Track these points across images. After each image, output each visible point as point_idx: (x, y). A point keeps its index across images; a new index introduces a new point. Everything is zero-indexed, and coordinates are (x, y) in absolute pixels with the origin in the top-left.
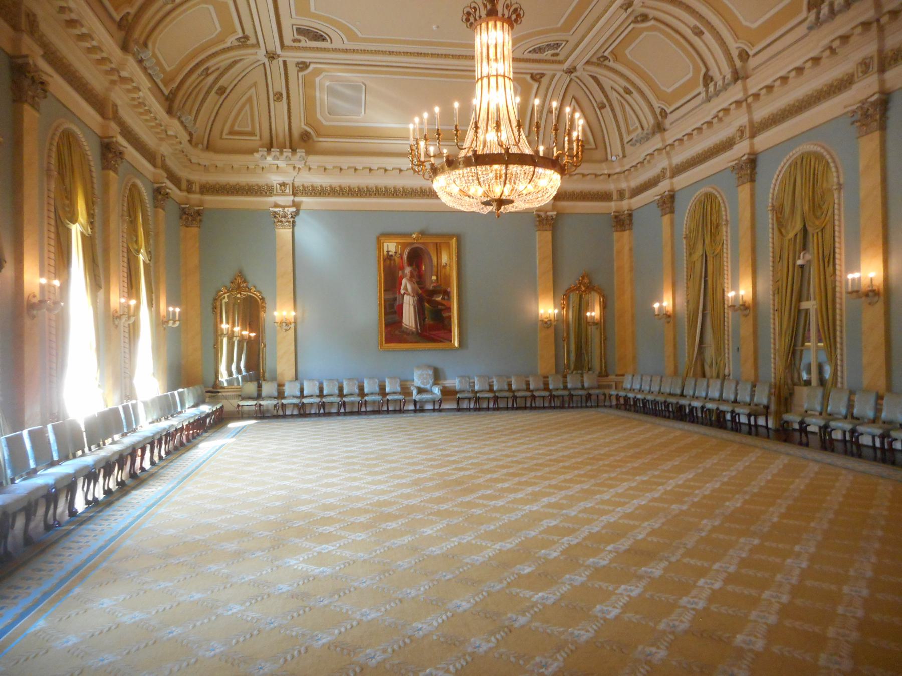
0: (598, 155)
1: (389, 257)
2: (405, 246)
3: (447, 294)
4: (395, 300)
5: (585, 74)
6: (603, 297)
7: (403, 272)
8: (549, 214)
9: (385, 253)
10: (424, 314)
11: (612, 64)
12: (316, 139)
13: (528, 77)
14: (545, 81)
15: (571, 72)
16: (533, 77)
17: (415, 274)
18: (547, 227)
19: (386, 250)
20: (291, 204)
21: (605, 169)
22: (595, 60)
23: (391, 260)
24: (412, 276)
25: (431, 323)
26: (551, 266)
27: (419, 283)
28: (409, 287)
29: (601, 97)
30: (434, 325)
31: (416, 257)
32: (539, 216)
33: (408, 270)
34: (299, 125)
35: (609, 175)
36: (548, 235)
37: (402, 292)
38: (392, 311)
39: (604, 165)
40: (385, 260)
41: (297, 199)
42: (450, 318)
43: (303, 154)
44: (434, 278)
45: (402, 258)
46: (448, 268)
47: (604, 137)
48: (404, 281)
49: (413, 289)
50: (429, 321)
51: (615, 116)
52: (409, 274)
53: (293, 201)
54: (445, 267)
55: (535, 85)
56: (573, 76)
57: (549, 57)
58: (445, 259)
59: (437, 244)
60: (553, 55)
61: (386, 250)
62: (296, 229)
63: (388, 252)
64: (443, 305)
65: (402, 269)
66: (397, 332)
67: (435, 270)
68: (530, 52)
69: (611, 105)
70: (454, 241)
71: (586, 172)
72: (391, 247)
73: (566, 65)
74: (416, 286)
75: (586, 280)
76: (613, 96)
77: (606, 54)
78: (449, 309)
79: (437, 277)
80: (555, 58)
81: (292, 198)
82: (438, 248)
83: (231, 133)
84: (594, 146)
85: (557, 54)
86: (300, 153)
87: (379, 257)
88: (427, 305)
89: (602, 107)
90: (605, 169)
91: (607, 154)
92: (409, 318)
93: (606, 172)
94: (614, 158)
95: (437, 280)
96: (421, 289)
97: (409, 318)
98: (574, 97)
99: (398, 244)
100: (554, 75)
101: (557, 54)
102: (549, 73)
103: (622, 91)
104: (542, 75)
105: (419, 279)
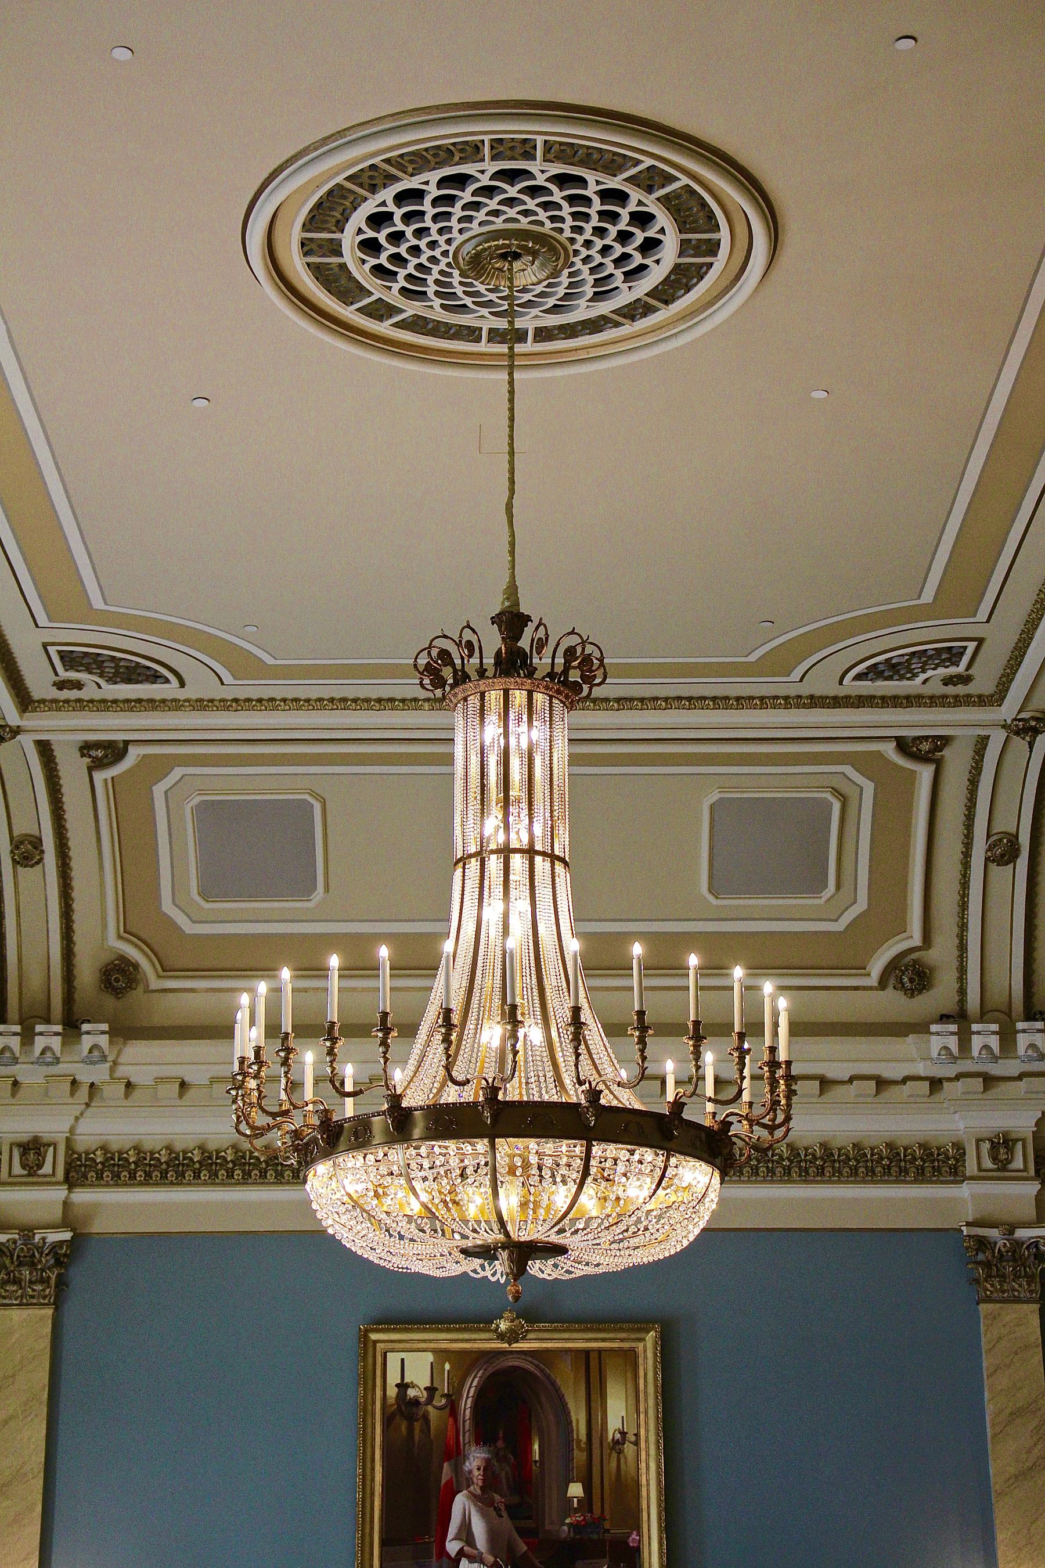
1: (405, 1408)
2: (467, 1362)
7: (457, 1469)
8: (1021, 1233)
9: (392, 1392)
12: (155, 984)
13: (889, 749)
14: (957, 762)
16: (903, 745)
17: (504, 1472)
18: (1021, 1287)
19: (393, 1378)
20: (58, 1214)
23: (411, 1419)
24: (490, 1481)
27: (514, 1511)
28: (479, 1528)
31: (511, 1402)
32: (982, 1243)
33: (475, 1460)
34: (101, 937)
37: (453, 1547)
40: (388, 1421)
41: (82, 1196)
43: (103, 1040)
44: (576, 1490)
46: (629, 1449)
48: (460, 1503)
53: (66, 1204)
54: (618, 1445)
55: (925, 773)
57: (936, 688)
58: (616, 1412)
59: (587, 1353)
60: (948, 681)
61: (393, 1378)
63: (403, 1386)
65: (455, 1454)
67: (579, 1456)
68: (859, 677)
70: (648, 1345)
72: (413, 1365)
73: (1008, 710)
74: (506, 1523)
79: (588, 1488)
80: (960, 690)
81: (60, 1193)
82: (592, 1368)
85: (965, 679)
86: (94, 1035)
87: (365, 1411)
96: (522, 1532)
99: (442, 1355)
100: (983, 742)
101: (965, 679)
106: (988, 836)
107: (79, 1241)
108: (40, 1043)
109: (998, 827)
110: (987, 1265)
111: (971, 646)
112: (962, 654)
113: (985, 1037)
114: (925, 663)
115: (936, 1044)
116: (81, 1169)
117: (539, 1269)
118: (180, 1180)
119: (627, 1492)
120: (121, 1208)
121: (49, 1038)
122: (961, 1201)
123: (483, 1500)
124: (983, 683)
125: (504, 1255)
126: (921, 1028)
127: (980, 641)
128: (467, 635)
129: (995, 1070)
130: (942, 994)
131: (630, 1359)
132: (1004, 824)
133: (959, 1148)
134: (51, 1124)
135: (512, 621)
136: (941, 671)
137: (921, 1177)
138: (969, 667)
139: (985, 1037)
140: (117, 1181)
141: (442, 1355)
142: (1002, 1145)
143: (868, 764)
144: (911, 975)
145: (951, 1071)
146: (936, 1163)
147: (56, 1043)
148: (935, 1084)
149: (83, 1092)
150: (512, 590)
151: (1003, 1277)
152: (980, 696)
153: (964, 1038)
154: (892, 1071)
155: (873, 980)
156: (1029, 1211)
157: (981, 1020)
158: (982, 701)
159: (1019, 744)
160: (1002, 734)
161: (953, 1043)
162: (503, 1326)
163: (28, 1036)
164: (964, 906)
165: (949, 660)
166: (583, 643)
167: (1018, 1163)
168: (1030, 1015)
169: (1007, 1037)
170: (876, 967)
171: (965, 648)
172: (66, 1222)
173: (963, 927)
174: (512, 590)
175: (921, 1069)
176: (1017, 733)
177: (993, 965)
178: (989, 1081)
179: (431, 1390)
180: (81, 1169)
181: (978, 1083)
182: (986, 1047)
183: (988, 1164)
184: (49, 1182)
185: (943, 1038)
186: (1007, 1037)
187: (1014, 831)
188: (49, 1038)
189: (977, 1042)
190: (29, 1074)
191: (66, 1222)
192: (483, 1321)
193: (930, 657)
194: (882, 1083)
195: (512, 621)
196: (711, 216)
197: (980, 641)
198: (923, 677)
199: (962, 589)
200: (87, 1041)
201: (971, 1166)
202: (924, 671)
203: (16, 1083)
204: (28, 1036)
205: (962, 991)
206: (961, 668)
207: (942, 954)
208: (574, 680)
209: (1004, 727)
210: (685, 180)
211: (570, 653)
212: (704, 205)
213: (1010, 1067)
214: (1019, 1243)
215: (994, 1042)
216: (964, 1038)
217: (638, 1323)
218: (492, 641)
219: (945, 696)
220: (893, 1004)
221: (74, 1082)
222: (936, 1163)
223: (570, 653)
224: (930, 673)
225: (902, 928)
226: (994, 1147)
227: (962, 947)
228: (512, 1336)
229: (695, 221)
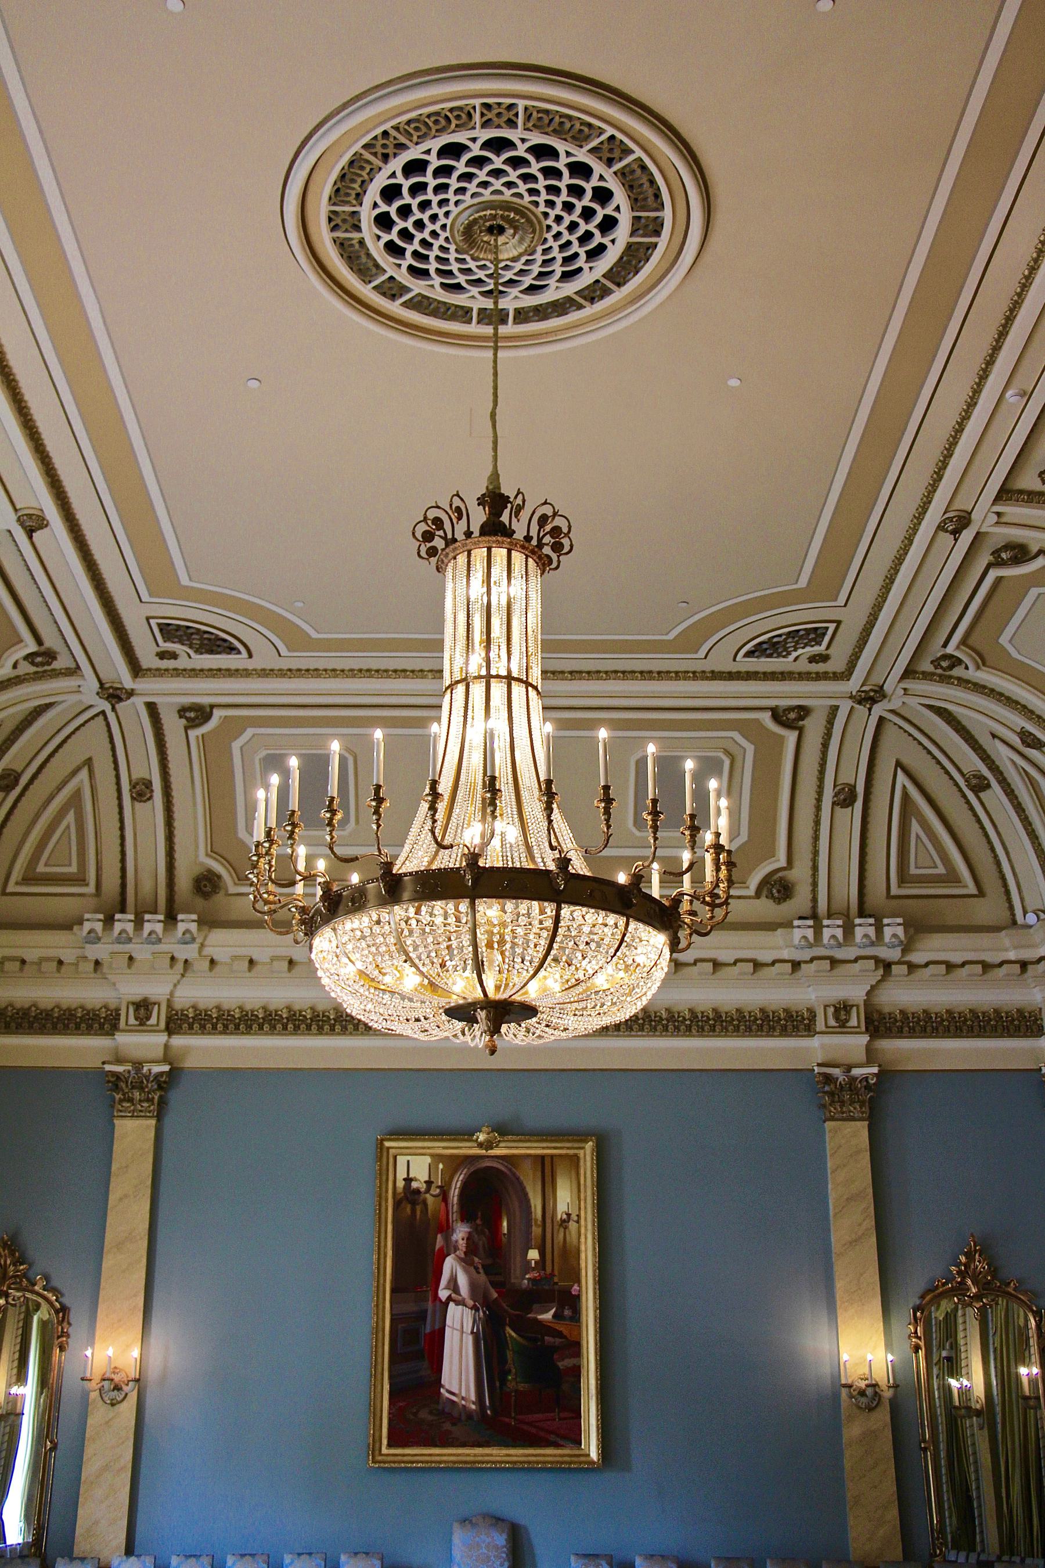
0: (987, 910)
1: (410, 1196)
2: (455, 1163)
3: (571, 1303)
4: (422, 1316)
5: (913, 702)
6: (1037, 1314)
7: (447, 1239)
8: (856, 1072)
9: (400, 1184)
10: (503, 1360)
11: (974, 674)
12: (233, 889)
13: (766, 717)
14: (814, 726)
15: (873, 701)
16: (778, 716)
17: (482, 1241)
18: (855, 1110)
19: (401, 1174)
21: (1006, 948)
22: (926, 666)
23: (414, 1203)
24: (472, 1249)
25: (522, 1387)
26: (871, 1223)
28: (463, 1281)
29: (973, 763)
30: (530, 1396)
31: (487, 1192)
32: (828, 1078)
33: (460, 1233)
34: (195, 855)
35: (1024, 965)
36: (858, 1133)
37: (443, 1294)
38: (415, 1347)
39: (1005, 938)
40: (397, 1204)
41: (179, 1041)
42: (576, 1372)
43: (193, 927)
44: (533, 1255)
45: (444, 1195)
46: (572, 1226)
47: (998, 864)
48: (449, 1264)
49: (473, 1286)
50: (514, 1382)
51: (1019, 808)
52: (462, 1244)
53: (166, 1046)
54: (564, 1223)
55: (792, 737)
56: (878, 710)
57: (803, 666)
58: (564, 1199)
59: (543, 1157)
60: (813, 659)
61: (401, 1174)
62: (167, 1121)
63: (408, 1180)
64: (560, 1334)
65: (446, 1229)
66: (424, 1414)
67: (536, 1231)
69: (1004, 782)
70: (587, 1151)
71: (957, 958)
72: (416, 1165)
73: (854, 685)
74: (482, 1278)
75: (980, 1265)
76: (1002, 754)
77: (950, 649)
78: (575, 1348)
79: (542, 1254)
80: (820, 667)
81: (163, 1038)
82: (546, 1169)
83: (29, 878)
84: (972, 889)
85: (824, 658)
86: (187, 923)
87: (381, 1197)
88: (509, 1330)
89: (979, 786)
90: (1006, 948)
91: (1011, 908)
92: (459, 1374)
93: (1012, 955)
94: (1031, 919)
95: (542, 1263)
97: (459, 1374)
98: (898, 764)
99: (437, 1158)
100: (834, 709)
101: (824, 658)
103: (1016, 741)
104: (804, 712)
105: (490, 1256)
106: (835, 786)
107: (175, 1074)
108: (147, 927)
110: (831, 1094)
111: (832, 627)
112: (824, 634)
113: (832, 930)
114: (797, 643)
115: (797, 934)
116: (178, 1022)
117: (512, 1033)
118: (248, 1031)
119: (570, 1257)
120: (202, 1050)
121: (154, 924)
122: (813, 1050)
123: (466, 1261)
124: (837, 664)
125: (481, 1015)
126: (789, 925)
127: (839, 623)
128: (457, 502)
129: (840, 954)
131: (574, 1162)
132: (847, 778)
133: (812, 1013)
134: (157, 989)
135: (495, 500)
136: (808, 649)
137: (784, 1032)
138: (828, 648)
139: (832, 930)
140: (203, 1031)
141: (437, 1158)
142: (842, 1010)
144: (778, 888)
145: (807, 955)
146: (795, 1023)
147: (159, 928)
148: (796, 965)
149: (180, 966)
150: (495, 477)
151: (842, 1103)
152: (834, 673)
153: (818, 929)
154: (766, 957)
155: (751, 892)
156: (862, 1057)
157: (829, 916)
158: (836, 677)
159: (861, 710)
161: (810, 933)
162: (482, 1137)
163: (139, 923)
164: (816, 838)
166: (555, 514)
167: (853, 1022)
168: (862, 914)
169: (849, 930)
170: (754, 881)
171: (827, 628)
172: (166, 1059)
173: (816, 853)
174: (495, 477)
175: (785, 954)
176: (860, 703)
177: (835, 882)
178: (834, 962)
179: (429, 1183)
180: (178, 1022)
182: (833, 937)
183: (832, 1022)
184: (154, 1031)
185: (802, 932)
186: (849, 930)
187: (853, 783)
188: (154, 924)
189: (827, 933)
190: (142, 952)
191: (166, 1059)
192: (467, 1134)
194: (757, 965)
195: (495, 500)
196: (657, 195)
197: (839, 623)
198: (794, 654)
199: (826, 582)
200: (181, 927)
201: (820, 1025)
202: (795, 650)
203: (131, 958)
204: (139, 923)
205: (815, 900)
206: (821, 649)
207: (800, 874)
208: (547, 547)
209: (851, 697)
210: (639, 153)
211: (543, 520)
212: (652, 182)
214: (854, 1079)
215: (839, 933)
216: (818, 929)
217: (579, 1136)
218: (479, 516)
219: (809, 673)
220: (766, 908)
221: (173, 958)
222: (795, 1023)
223: (543, 520)
224: (800, 651)
225: (772, 854)
227: (815, 868)
228: (488, 1145)
229: (645, 199)
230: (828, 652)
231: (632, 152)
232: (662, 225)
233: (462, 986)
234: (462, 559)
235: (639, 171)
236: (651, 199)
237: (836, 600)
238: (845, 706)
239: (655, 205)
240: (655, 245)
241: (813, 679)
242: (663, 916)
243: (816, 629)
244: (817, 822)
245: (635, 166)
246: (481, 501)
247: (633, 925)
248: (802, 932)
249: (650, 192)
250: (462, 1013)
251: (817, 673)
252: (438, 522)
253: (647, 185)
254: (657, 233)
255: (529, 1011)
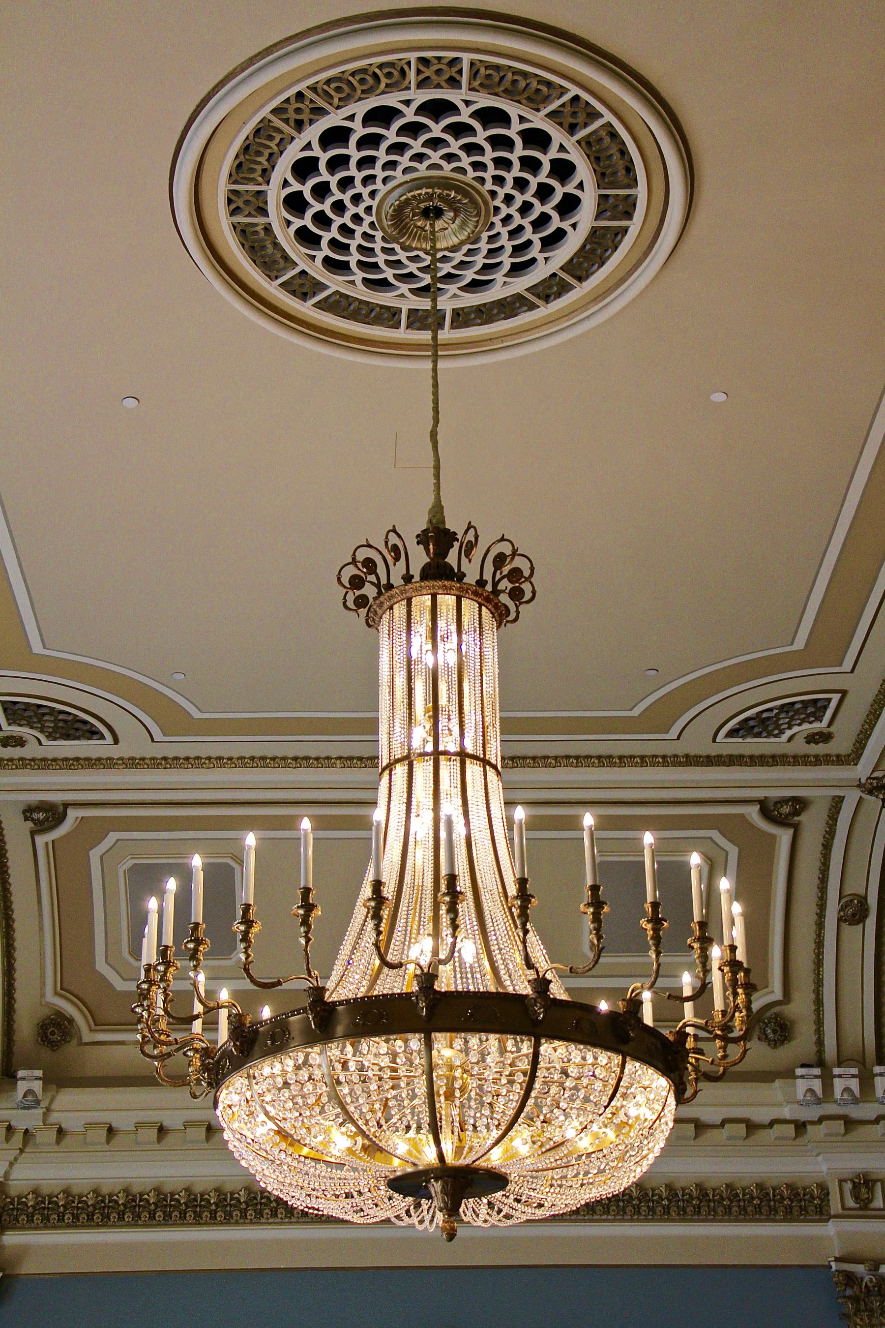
13: (753, 813)
14: (812, 823)
16: (767, 809)
32: (850, 1279)
55: (784, 837)
57: (800, 747)
60: (811, 739)
68: (732, 733)
73: (863, 769)
80: (820, 749)
85: (824, 737)
100: (838, 802)
101: (824, 737)
102: (819, 796)
104: (799, 804)
109: (848, 891)
110: (855, 1300)
111: (836, 697)
112: (825, 708)
113: (845, 1082)
114: (792, 718)
115: (801, 1086)
117: (476, 1212)
124: (841, 745)
125: (436, 1187)
126: (788, 1074)
127: (844, 693)
128: (393, 539)
130: (802, 1042)
132: (855, 887)
135: (438, 537)
136: (806, 726)
137: (789, 1216)
138: (830, 724)
139: (845, 1082)
140: (46, 1224)
143: (733, 828)
145: (814, 1113)
146: (800, 1203)
148: (800, 1127)
149: (18, 1138)
150: (438, 509)
152: (838, 756)
153: (827, 1080)
154: (761, 1115)
158: (840, 760)
160: (856, 794)
164: (819, 963)
165: (813, 714)
166: (515, 553)
169: (866, 1081)
171: (829, 700)
173: (819, 983)
174: (438, 509)
175: (786, 1112)
176: (870, 793)
177: (846, 1022)
178: (850, 1123)
181: (839, 1126)
182: (847, 1090)
183: (850, 1203)
185: (807, 1083)
186: (866, 1081)
187: (862, 892)
189: (839, 1085)
193: (797, 712)
194: (752, 1127)
195: (438, 537)
196: (629, 169)
197: (844, 693)
198: (788, 733)
199: (829, 643)
200: (22, 1087)
201: (835, 1206)
202: (790, 728)
205: (820, 1042)
207: (800, 1008)
208: (504, 593)
209: (860, 786)
211: (500, 560)
212: (624, 152)
213: (868, 1111)
215: (854, 1084)
216: (827, 1080)
218: (419, 558)
219: (807, 756)
221: (10, 1129)
223: (500, 560)
224: (796, 729)
226: (856, 1187)
227: (819, 1002)
229: (614, 174)
230: (831, 729)
231: (600, 115)
232: (634, 205)
233: (411, 1149)
234: (400, 610)
235: (607, 140)
236: (622, 173)
237: (841, 665)
238: (852, 797)
239: (626, 181)
240: (625, 230)
241: (811, 764)
242: (666, 1055)
243: (816, 701)
244: (819, 944)
245: (603, 133)
246: (423, 539)
247: (633, 1066)
248: (807, 1083)
249: (621, 164)
250: (410, 1184)
251: (817, 757)
252: (369, 564)
253: (616, 156)
254: (629, 215)
255: (496, 1180)
